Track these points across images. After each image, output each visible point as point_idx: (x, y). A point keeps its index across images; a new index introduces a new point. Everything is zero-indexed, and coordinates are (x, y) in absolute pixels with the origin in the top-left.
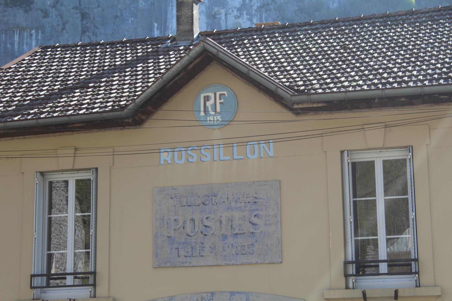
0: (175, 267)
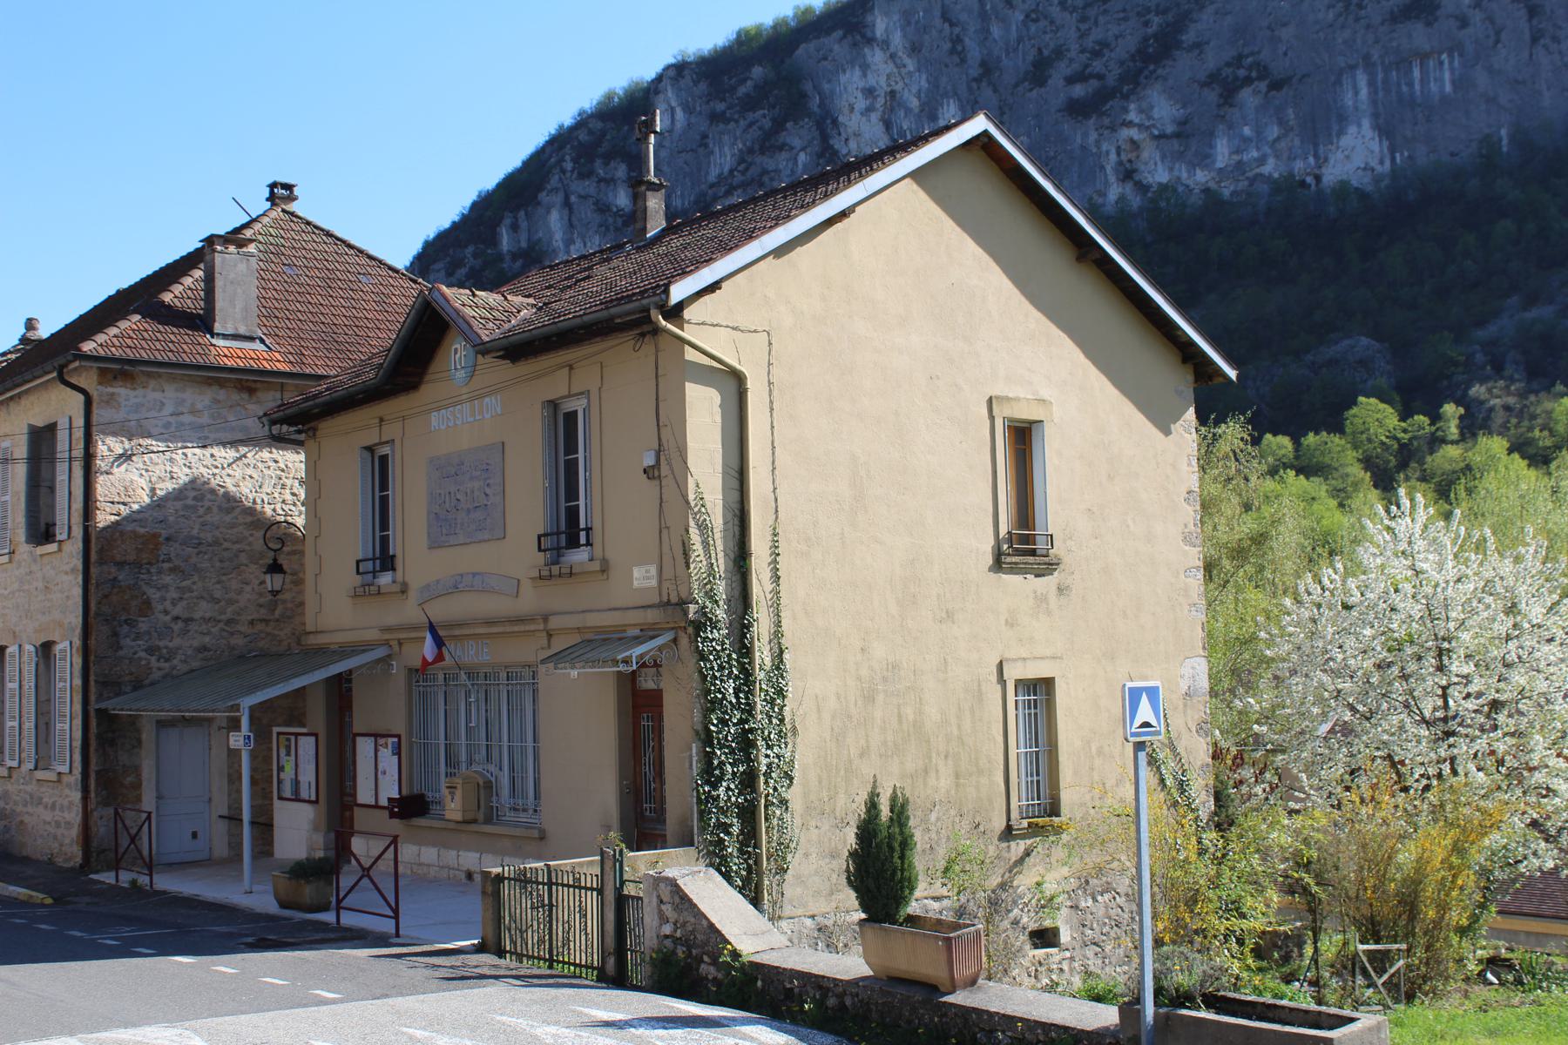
0: (440, 547)
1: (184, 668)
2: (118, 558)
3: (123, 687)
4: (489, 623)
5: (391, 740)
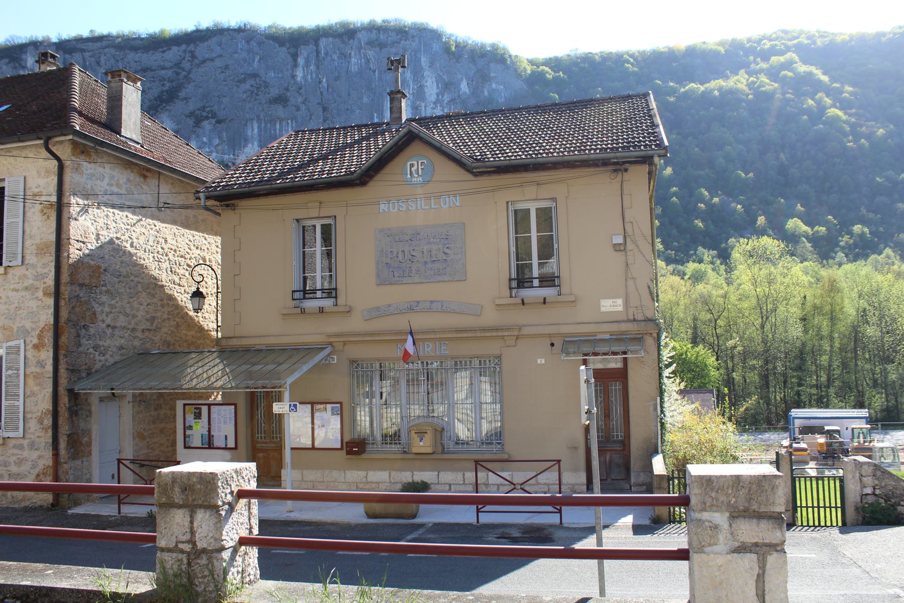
1: (111, 361)
2: (81, 281)
3: (82, 374)
4: (458, 331)
5: (329, 406)
